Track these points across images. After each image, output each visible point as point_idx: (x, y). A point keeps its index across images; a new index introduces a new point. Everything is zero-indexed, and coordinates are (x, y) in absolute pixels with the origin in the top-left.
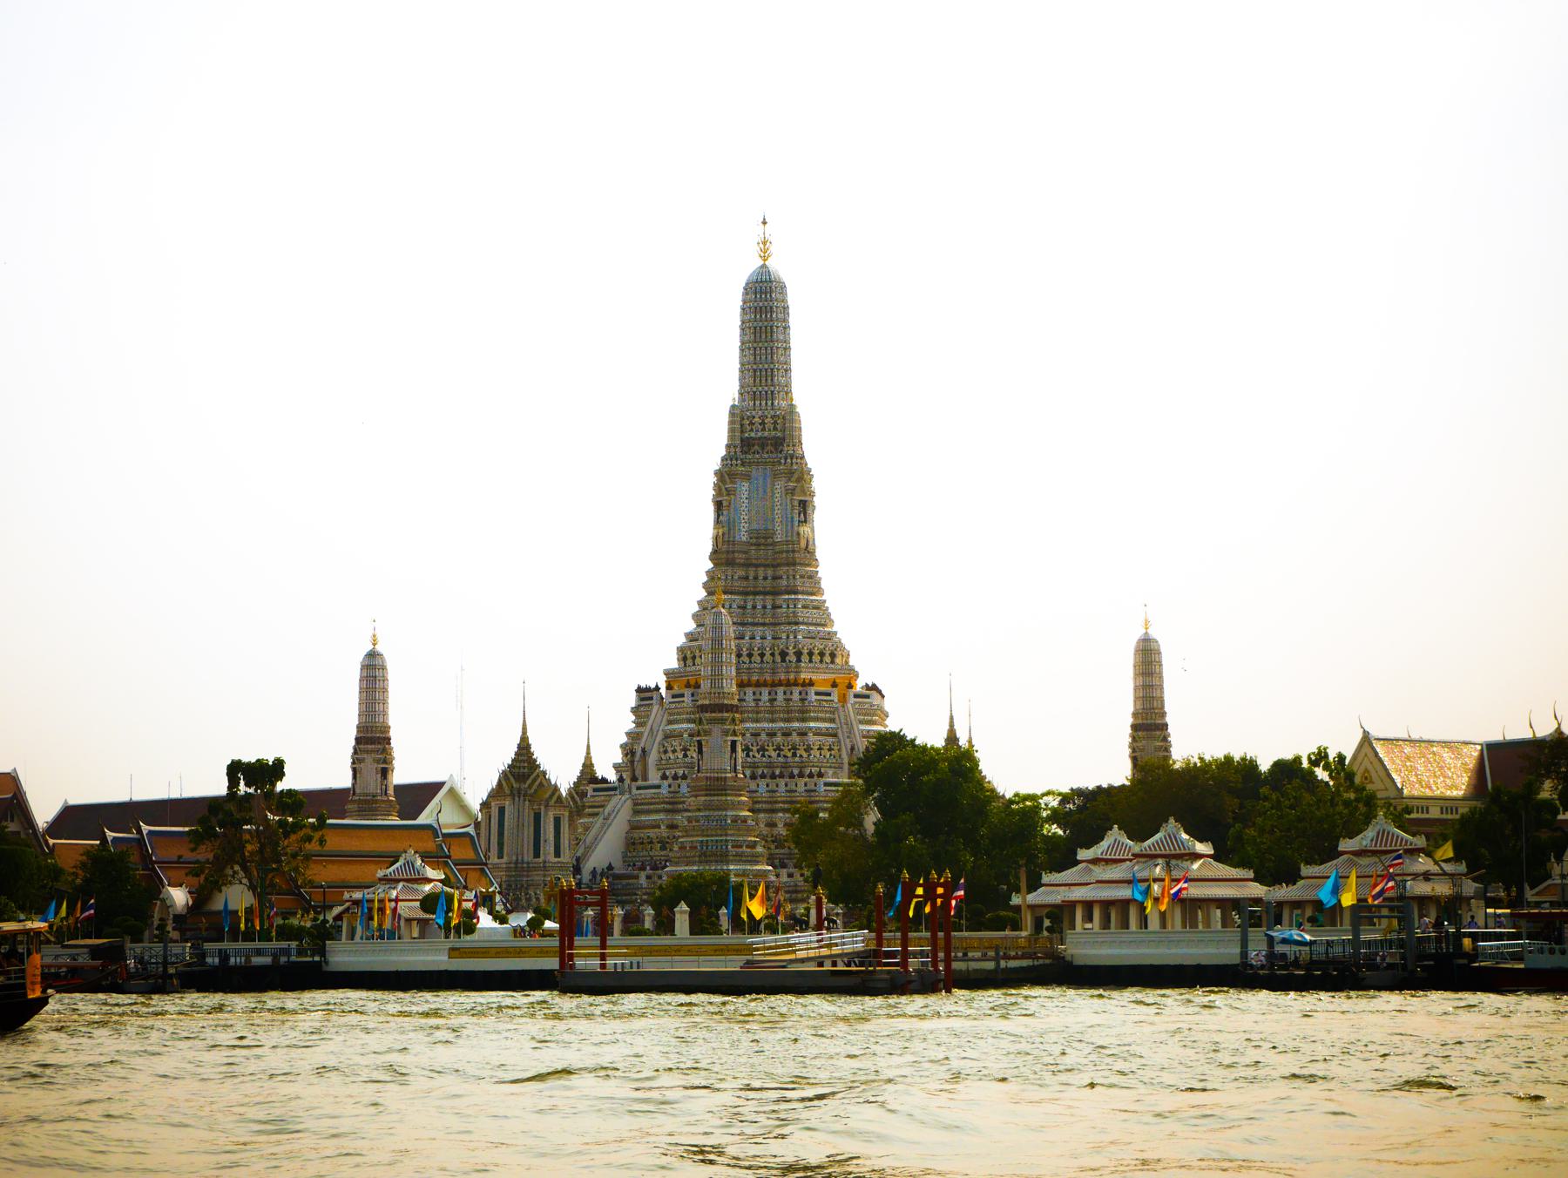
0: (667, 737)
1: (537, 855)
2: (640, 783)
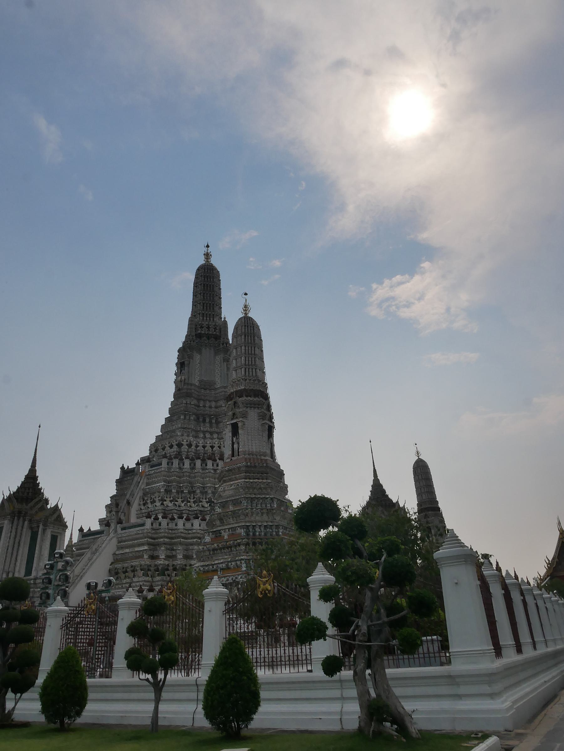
0: (145, 494)
1: (28, 571)
2: (124, 525)
